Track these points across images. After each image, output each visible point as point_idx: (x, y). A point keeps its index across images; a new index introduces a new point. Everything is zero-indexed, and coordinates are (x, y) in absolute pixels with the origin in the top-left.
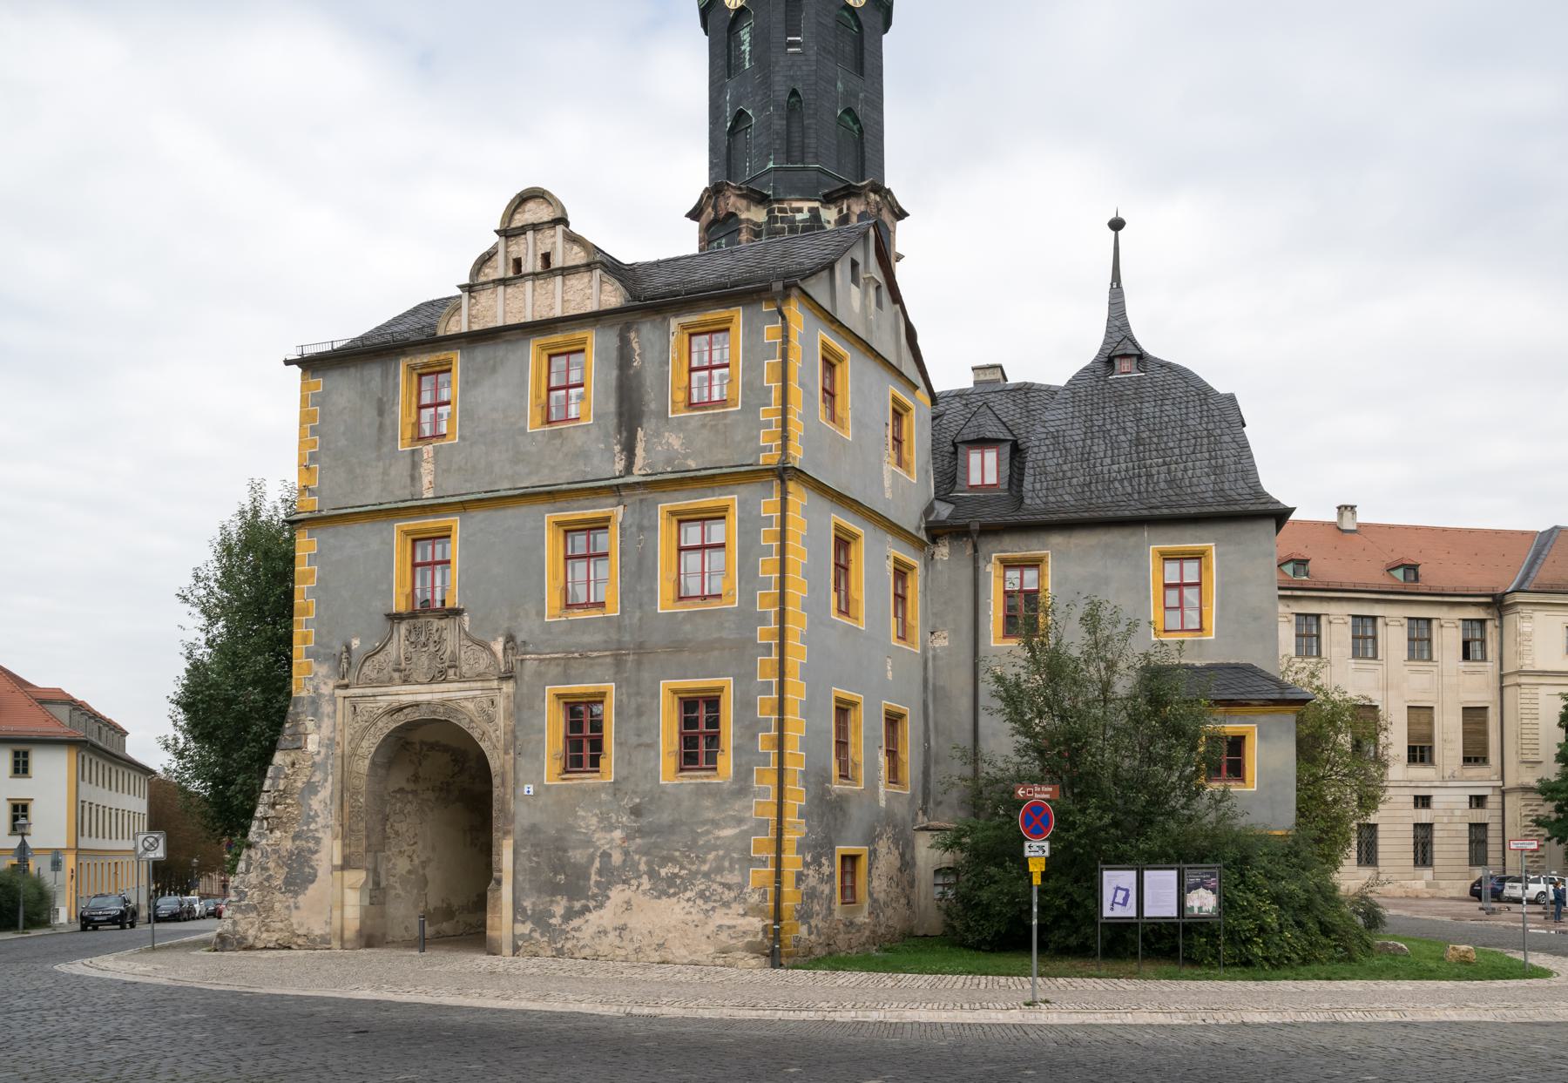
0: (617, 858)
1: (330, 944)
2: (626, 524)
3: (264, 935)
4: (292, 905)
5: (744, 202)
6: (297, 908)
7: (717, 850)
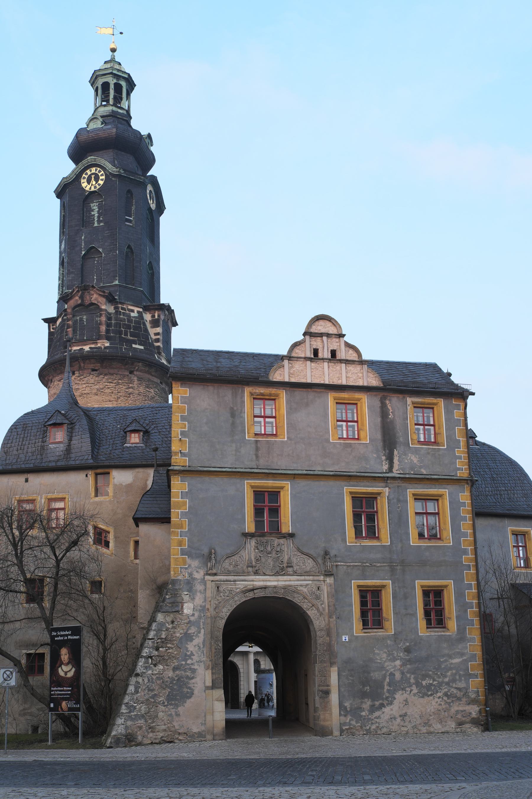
0: (398, 676)
1: (205, 737)
2: (391, 497)
3: (151, 735)
4: (173, 713)
5: (104, 300)
6: (178, 715)
7: (452, 670)
